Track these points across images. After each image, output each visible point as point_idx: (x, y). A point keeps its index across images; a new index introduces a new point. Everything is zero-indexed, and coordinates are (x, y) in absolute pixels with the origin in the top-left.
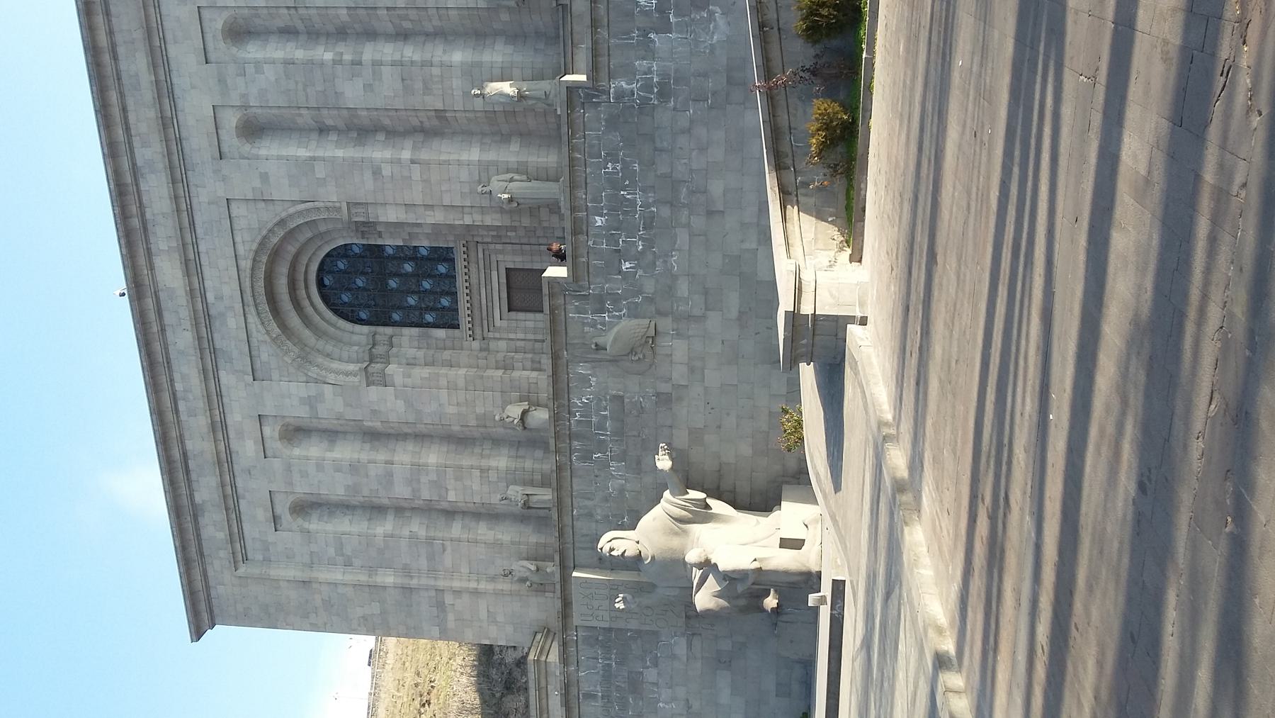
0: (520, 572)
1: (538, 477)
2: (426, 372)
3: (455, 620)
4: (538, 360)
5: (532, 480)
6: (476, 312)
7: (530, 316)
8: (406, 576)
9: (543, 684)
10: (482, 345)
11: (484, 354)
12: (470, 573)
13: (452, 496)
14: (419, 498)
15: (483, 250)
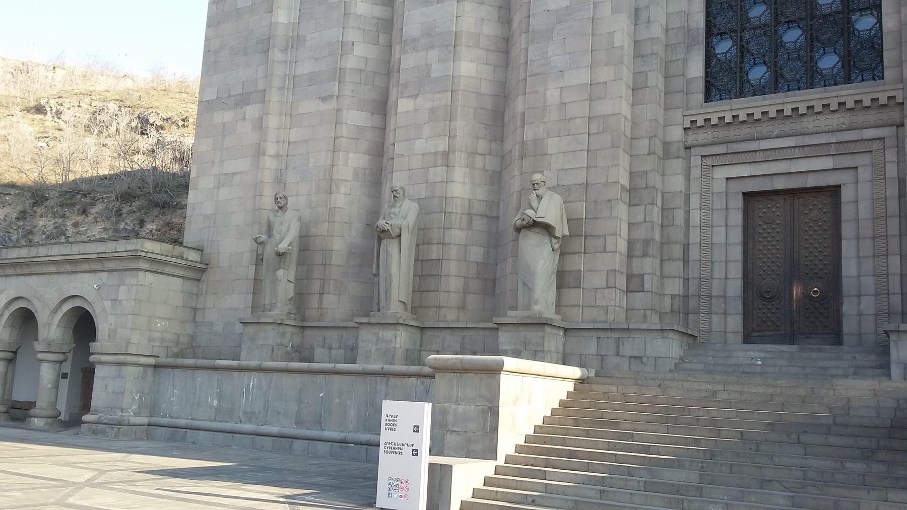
0: (281, 223)
1: (435, 252)
2: (623, 40)
3: (224, 123)
4: (650, 252)
5: (429, 243)
6: (744, 131)
7: (737, 235)
8: (287, 42)
9: (110, 265)
10: (675, 146)
11: (660, 151)
12: (289, 143)
13: (404, 105)
14: (403, 51)
15: (882, 139)
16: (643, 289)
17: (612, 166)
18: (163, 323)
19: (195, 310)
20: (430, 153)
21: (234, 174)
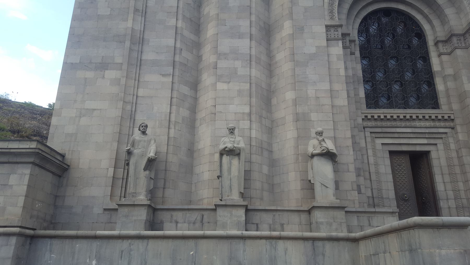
6: (389, 124)
7: (389, 170)
15: (446, 133)
16: (361, 192)
17: (347, 130)
18: (40, 205)
19: (56, 197)
20: (240, 113)
21: (95, 109)
